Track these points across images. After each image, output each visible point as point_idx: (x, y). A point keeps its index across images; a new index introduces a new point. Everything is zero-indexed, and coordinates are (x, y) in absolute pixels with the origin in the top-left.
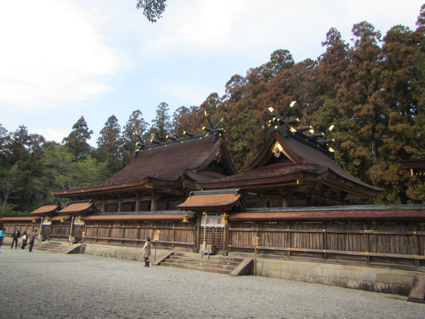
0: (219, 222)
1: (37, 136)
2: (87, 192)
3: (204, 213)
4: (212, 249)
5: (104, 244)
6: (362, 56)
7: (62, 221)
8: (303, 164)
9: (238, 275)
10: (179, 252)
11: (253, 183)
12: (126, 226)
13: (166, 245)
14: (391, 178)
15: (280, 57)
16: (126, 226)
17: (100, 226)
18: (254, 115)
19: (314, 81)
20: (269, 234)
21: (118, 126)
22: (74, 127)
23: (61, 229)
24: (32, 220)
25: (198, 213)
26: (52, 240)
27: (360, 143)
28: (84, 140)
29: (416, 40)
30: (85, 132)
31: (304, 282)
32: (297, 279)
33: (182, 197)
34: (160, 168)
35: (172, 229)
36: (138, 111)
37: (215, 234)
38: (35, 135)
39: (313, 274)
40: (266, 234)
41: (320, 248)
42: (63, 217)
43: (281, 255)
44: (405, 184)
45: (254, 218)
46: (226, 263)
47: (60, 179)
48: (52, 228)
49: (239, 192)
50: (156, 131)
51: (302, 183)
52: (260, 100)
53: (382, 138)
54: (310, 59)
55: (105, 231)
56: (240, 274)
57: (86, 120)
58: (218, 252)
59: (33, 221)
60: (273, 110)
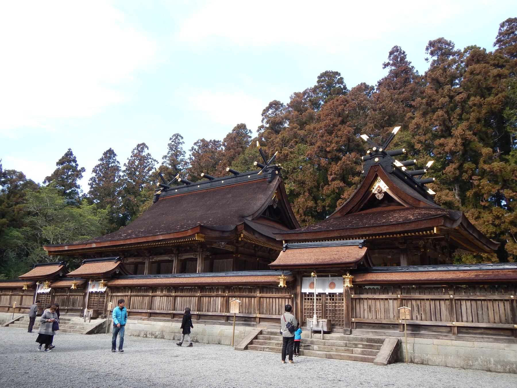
0: (332, 286)
1: (14, 172)
2: (101, 247)
3: (312, 274)
4: (327, 325)
6: (442, 79)
7: (73, 287)
8: (422, 208)
9: (387, 364)
10: (269, 330)
11: (365, 233)
12: (177, 294)
13: (247, 320)
14: (486, 229)
15: (330, 81)
16: (177, 294)
17: (132, 294)
18: (303, 151)
19: (380, 109)
20: (419, 302)
21: (116, 163)
22: (58, 164)
23: (68, 299)
24: (22, 287)
25: (298, 273)
27: (442, 186)
28: (74, 180)
29: (500, 64)
30: (75, 169)
31: (487, 371)
32: (474, 367)
33: (232, 253)
34: (219, 213)
35: (255, 297)
36: (144, 144)
37: (326, 303)
38: (12, 171)
39: (502, 359)
40: (414, 302)
41: (507, 322)
42: (74, 282)
43: (441, 332)
44: (502, 237)
45: (397, 281)
46: (356, 345)
47: (48, 231)
49: (364, 245)
50: (169, 171)
51: (439, 233)
52: (310, 131)
53: (471, 179)
54: (365, 83)
55: (143, 301)
56: (390, 362)
57: (75, 154)
58: (335, 330)
59: (24, 289)
60: (368, 138)
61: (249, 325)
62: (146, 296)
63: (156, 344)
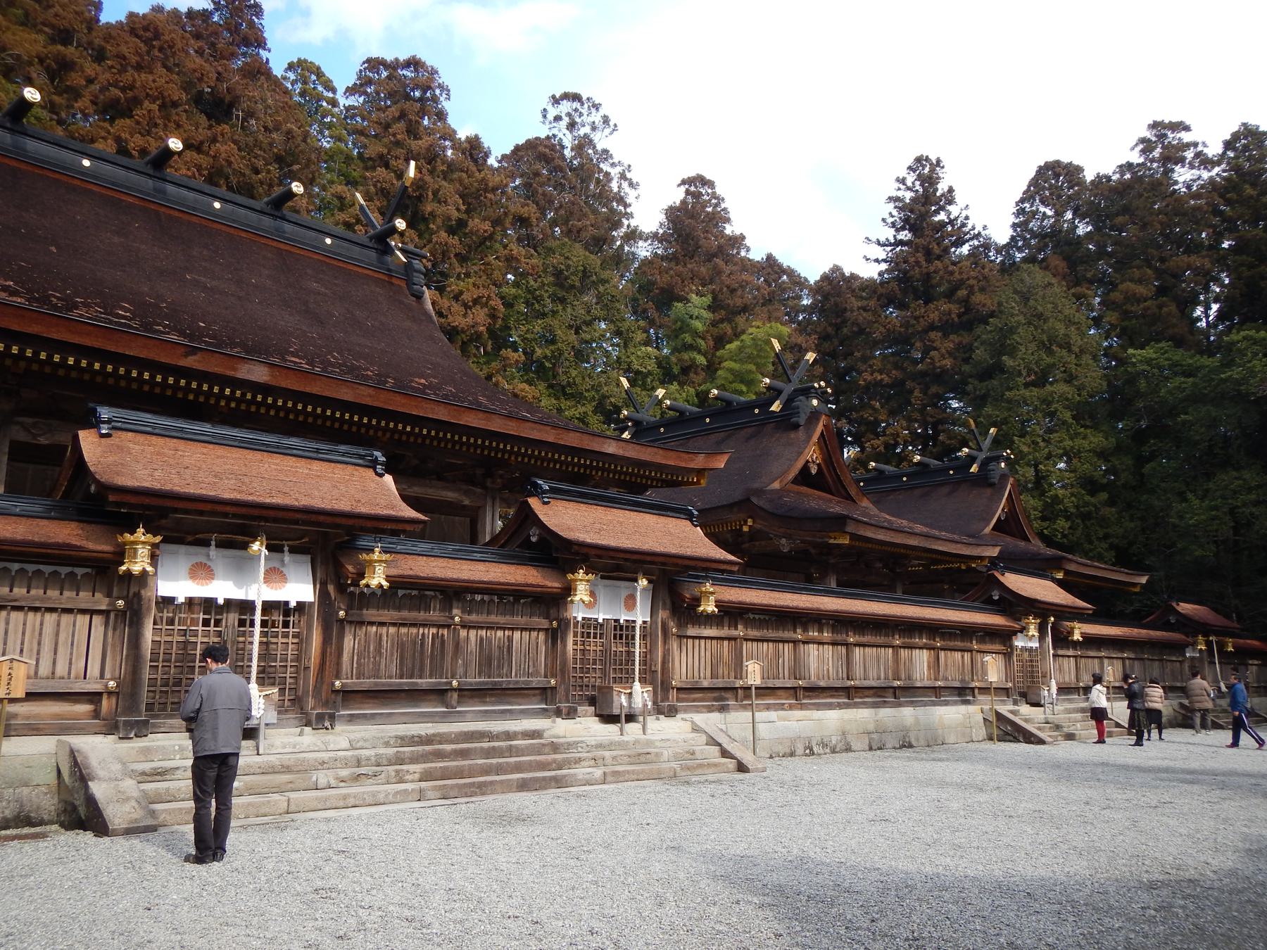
5: (781, 707)
11: (940, 548)
13: (963, 693)
26: (352, 719)
48: (332, 629)
55: (777, 655)
62: (784, 641)
63: (829, 769)
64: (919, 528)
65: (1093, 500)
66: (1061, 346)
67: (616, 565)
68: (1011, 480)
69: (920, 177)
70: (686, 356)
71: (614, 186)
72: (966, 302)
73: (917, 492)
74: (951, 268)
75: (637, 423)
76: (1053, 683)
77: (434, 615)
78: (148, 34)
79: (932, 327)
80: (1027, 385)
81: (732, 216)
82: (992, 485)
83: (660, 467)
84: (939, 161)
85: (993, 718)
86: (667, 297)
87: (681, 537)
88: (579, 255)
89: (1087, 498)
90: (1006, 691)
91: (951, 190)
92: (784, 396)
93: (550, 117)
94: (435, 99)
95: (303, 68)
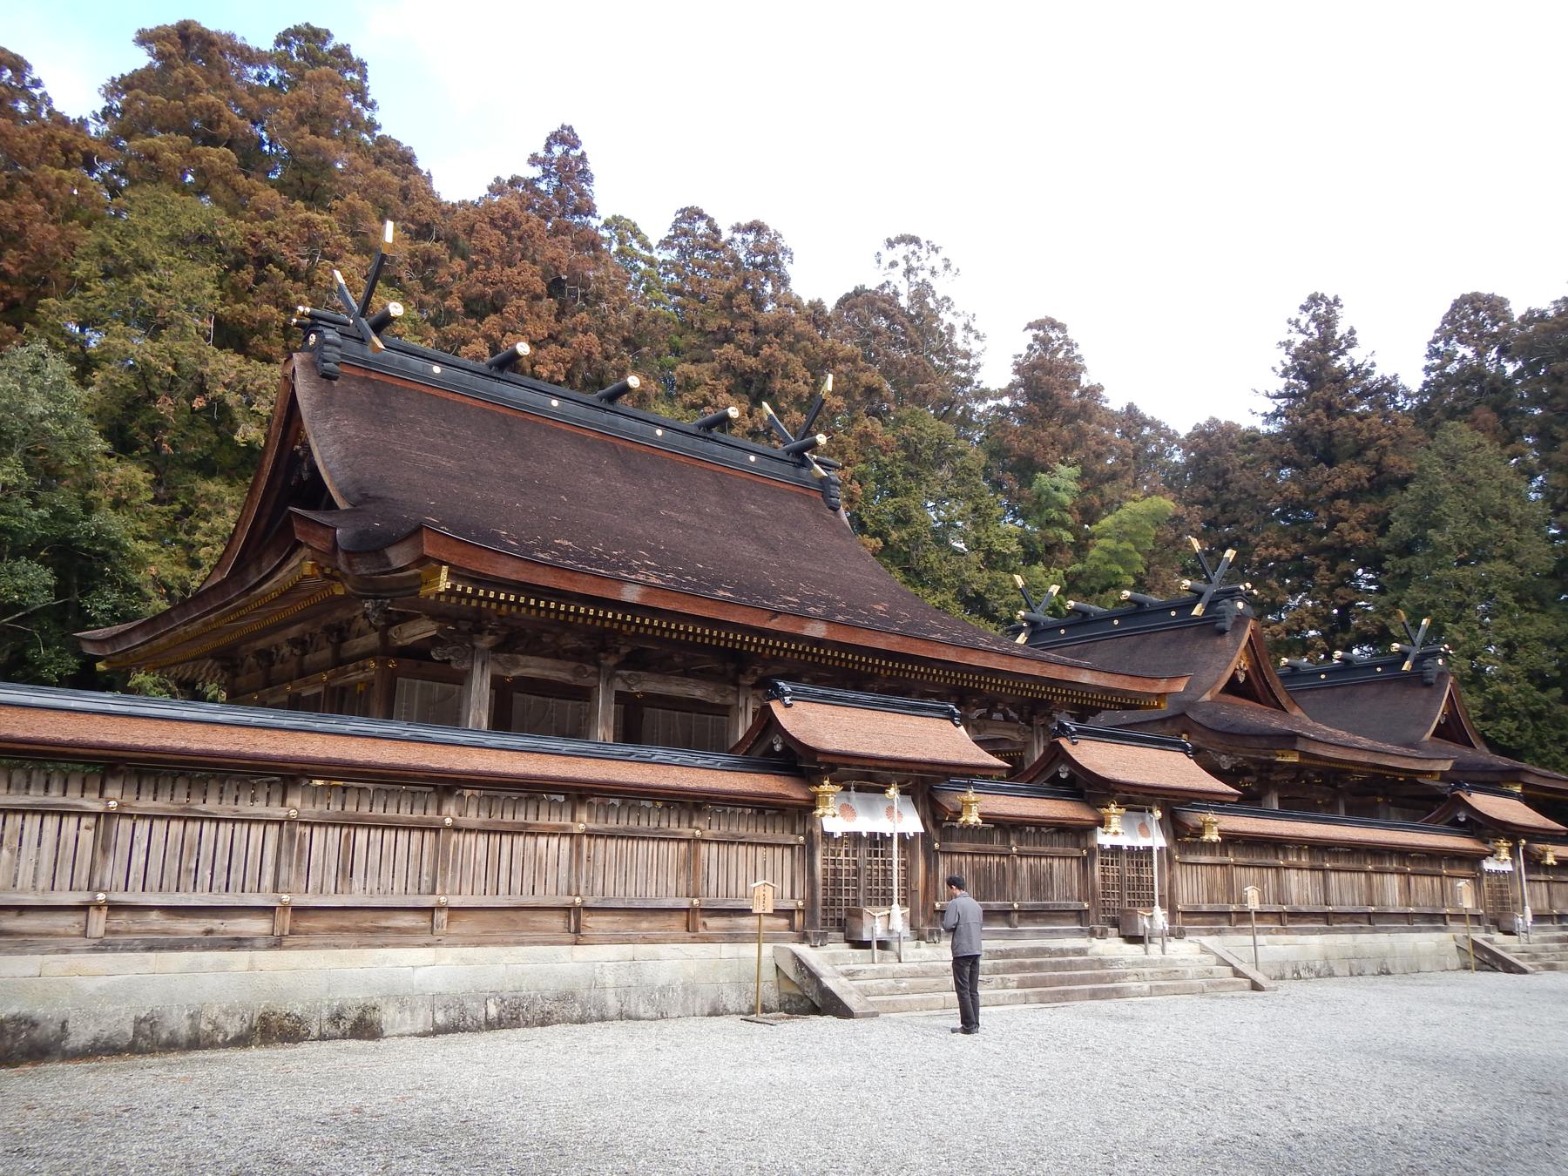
13: (1435, 919)
61: (1438, 929)
62: (1268, 867)
64: (1343, 735)
65: (1544, 697)
66: (1496, 517)
67: (1136, 798)
68: (1451, 679)
69: (1314, 318)
70: (1051, 533)
71: (958, 339)
72: (1378, 466)
73: (1338, 691)
74: (1358, 425)
75: (1033, 624)
76: (1528, 909)
77: (996, 846)
78: (509, 224)
79: (1337, 495)
80: (1462, 562)
81: (1086, 363)
82: (1429, 685)
83: (1125, 693)
84: (1336, 301)
85: (1468, 947)
86: (1027, 468)
87: (1172, 769)
88: (930, 424)
89: (1537, 694)
90: (1476, 918)
91: (1352, 332)
92: (1206, 598)
93: (886, 262)
94: (778, 264)
95: (616, 223)
